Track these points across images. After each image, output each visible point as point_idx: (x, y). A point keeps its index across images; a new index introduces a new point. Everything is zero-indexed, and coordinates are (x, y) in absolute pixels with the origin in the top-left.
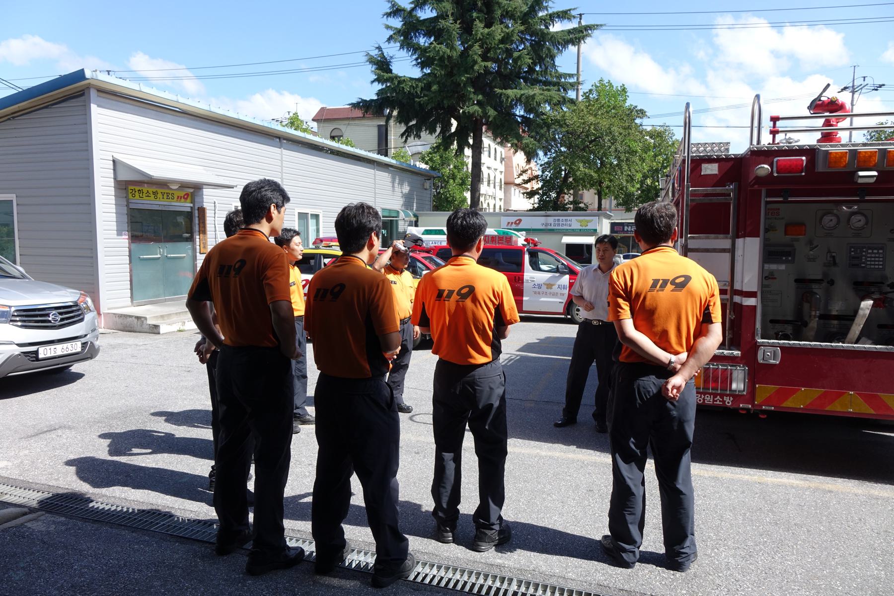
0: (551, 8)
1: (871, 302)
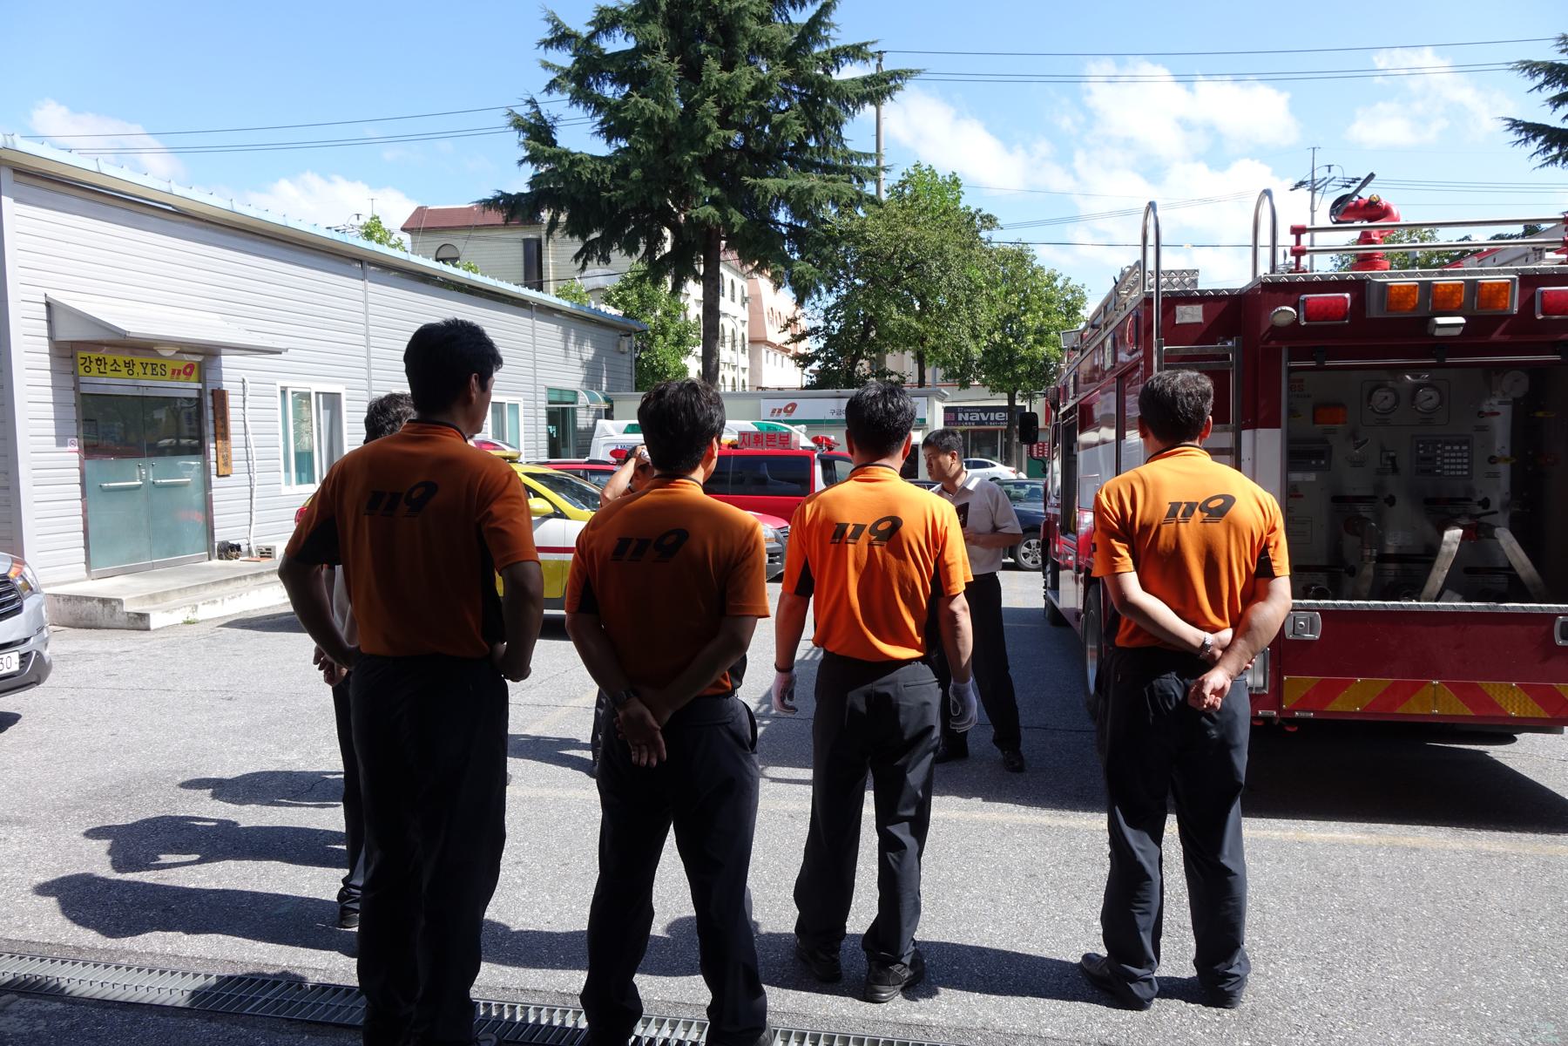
0: (833, 39)
1: (1460, 531)
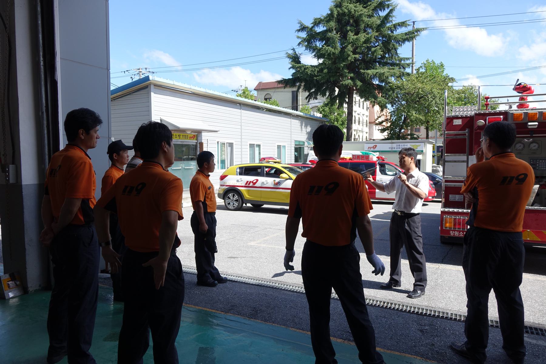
0: (394, 21)
1: (538, 186)
